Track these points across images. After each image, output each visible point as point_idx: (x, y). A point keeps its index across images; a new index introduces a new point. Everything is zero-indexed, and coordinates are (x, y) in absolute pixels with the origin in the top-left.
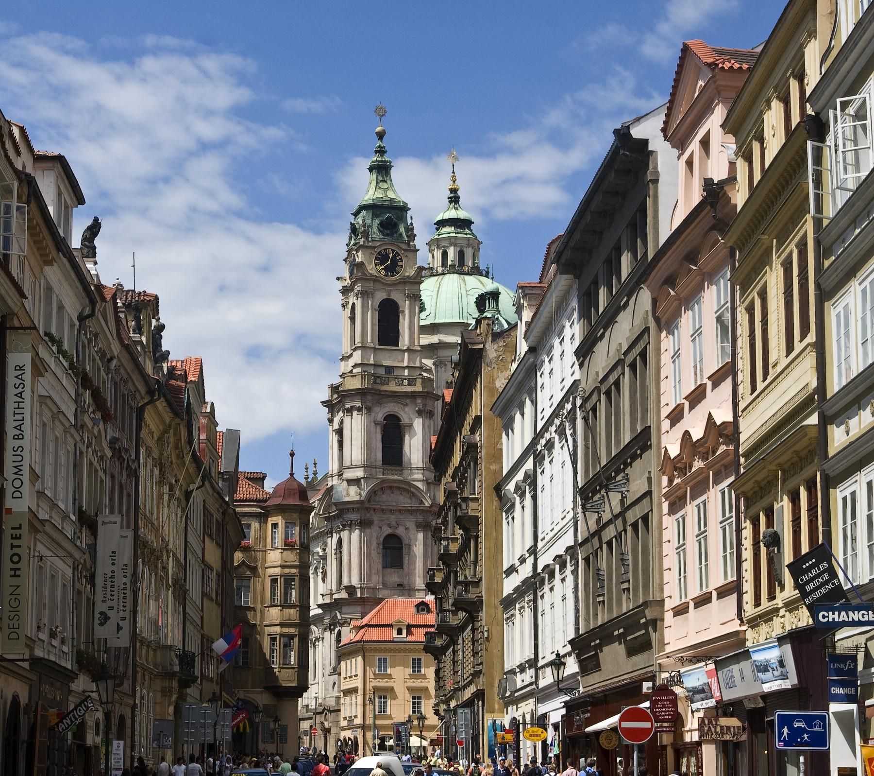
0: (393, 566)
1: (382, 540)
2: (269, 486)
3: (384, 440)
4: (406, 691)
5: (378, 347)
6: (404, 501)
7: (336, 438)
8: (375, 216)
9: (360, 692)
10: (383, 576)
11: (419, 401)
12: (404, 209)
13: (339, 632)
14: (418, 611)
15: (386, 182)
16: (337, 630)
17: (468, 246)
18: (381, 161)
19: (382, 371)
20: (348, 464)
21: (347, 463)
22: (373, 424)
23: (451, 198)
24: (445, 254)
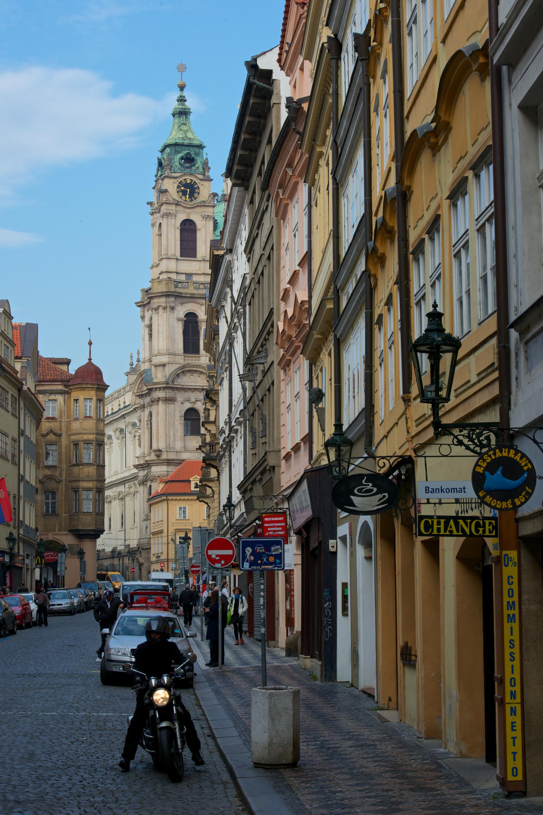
1: (183, 413)
2: (72, 369)
5: (179, 258)
7: (147, 331)
9: (165, 534)
10: (184, 442)
12: (201, 147)
13: (150, 486)
16: (149, 484)
18: (182, 109)
19: (183, 278)
20: (156, 352)
22: (175, 320)
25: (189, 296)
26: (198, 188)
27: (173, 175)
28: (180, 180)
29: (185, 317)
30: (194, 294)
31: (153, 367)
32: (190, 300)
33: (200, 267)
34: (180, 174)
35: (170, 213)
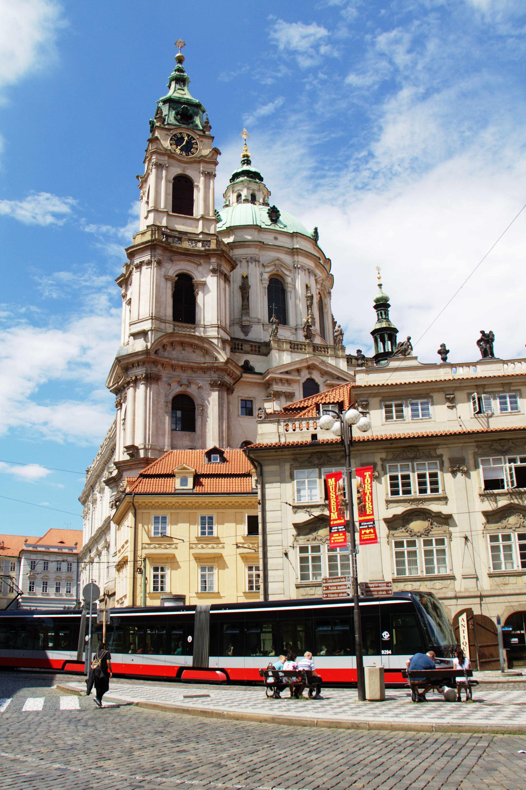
0: (183, 429)
1: (171, 398)
3: (176, 296)
4: (192, 558)
5: (171, 213)
6: (197, 358)
10: (172, 439)
11: (213, 260)
14: (210, 460)
15: (183, 90)
17: (259, 190)
18: (180, 75)
22: (163, 279)
23: (244, 161)
24: (239, 196)
25: (182, 251)
27: (167, 127)
28: (174, 133)
29: (176, 276)
31: (132, 338)
35: (161, 165)
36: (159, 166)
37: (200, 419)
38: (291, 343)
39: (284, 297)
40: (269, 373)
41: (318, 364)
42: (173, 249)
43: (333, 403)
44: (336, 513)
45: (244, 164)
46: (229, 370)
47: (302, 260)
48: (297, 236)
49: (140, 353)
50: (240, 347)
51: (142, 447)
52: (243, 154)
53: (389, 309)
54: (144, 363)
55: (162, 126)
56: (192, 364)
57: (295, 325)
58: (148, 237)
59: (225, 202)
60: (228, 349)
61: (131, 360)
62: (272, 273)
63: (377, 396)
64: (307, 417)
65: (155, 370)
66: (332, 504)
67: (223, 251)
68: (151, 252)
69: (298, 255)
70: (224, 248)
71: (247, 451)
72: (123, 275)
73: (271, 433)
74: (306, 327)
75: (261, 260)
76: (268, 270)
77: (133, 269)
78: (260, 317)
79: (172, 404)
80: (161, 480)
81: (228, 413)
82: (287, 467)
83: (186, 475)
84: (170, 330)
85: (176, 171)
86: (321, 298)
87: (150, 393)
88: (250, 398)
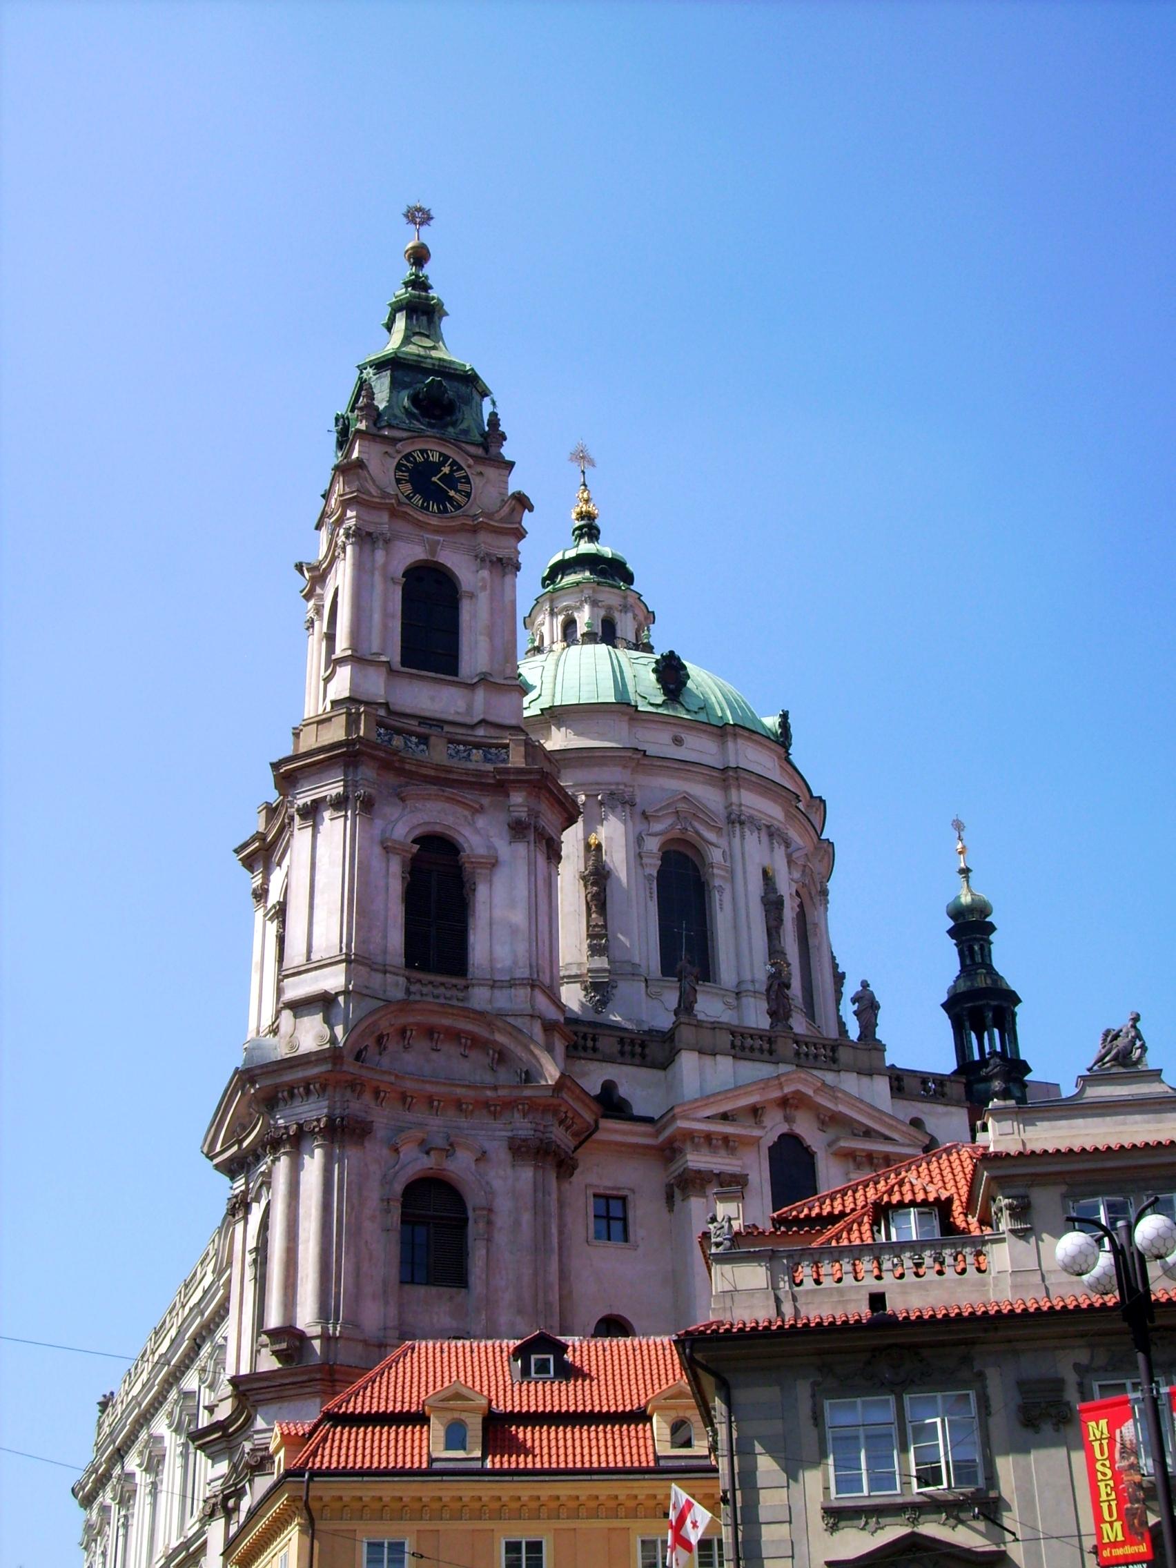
1: (399, 1188)
7: (272, 928)
8: (395, 385)
10: (401, 1306)
14: (525, 1372)
15: (428, 337)
17: (625, 608)
18: (419, 297)
21: (296, 954)
22: (377, 850)
23: (580, 528)
24: (570, 625)
25: (432, 773)
26: (467, 480)
29: (415, 841)
30: (449, 770)
31: (287, 1015)
32: (433, 789)
33: (470, 708)
34: (405, 434)
35: (369, 534)
36: (364, 538)
37: (484, 1252)
38: (733, 1034)
39: (703, 904)
40: (674, 1118)
41: (810, 1093)
42: (407, 767)
43: (925, 1203)
44: (1118, 1525)
45: (581, 536)
46: (563, 1109)
47: (752, 801)
48: (735, 736)
49: (313, 1058)
50: (590, 1043)
51: (317, 1330)
52: (578, 510)
53: (992, 937)
54: (324, 1088)
55: (374, 431)
56: (459, 1091)
57: (735, 984)
58: (336, 732)
59: (533, 641)
60: (560, 1047)
61: (289, 1077)
62: (669, 836)
63: (1055, 1184)
64: (846, 1243)
65: (355, 1107)
66: (1103, 1497)
67: (545, 775)
68: (346, 775)
69: (739, 787)
70: (547, 768)
71: (687, 1344)
72: (260, 837)
73: (751, 1292)
74: (775, 987)
75: (638, 800)
76: (658, 827)
77: (292, 818)
78: (637, 960)
79: (403, 1206)
80: (387, 1433)
81: (561, 1233)
82: (803, 1390)
83: (464, 1416)
84: (399, 994)
85: (409, 553)
86: (801, 906)
87: (341, 1173)
88: (619, 1189)
